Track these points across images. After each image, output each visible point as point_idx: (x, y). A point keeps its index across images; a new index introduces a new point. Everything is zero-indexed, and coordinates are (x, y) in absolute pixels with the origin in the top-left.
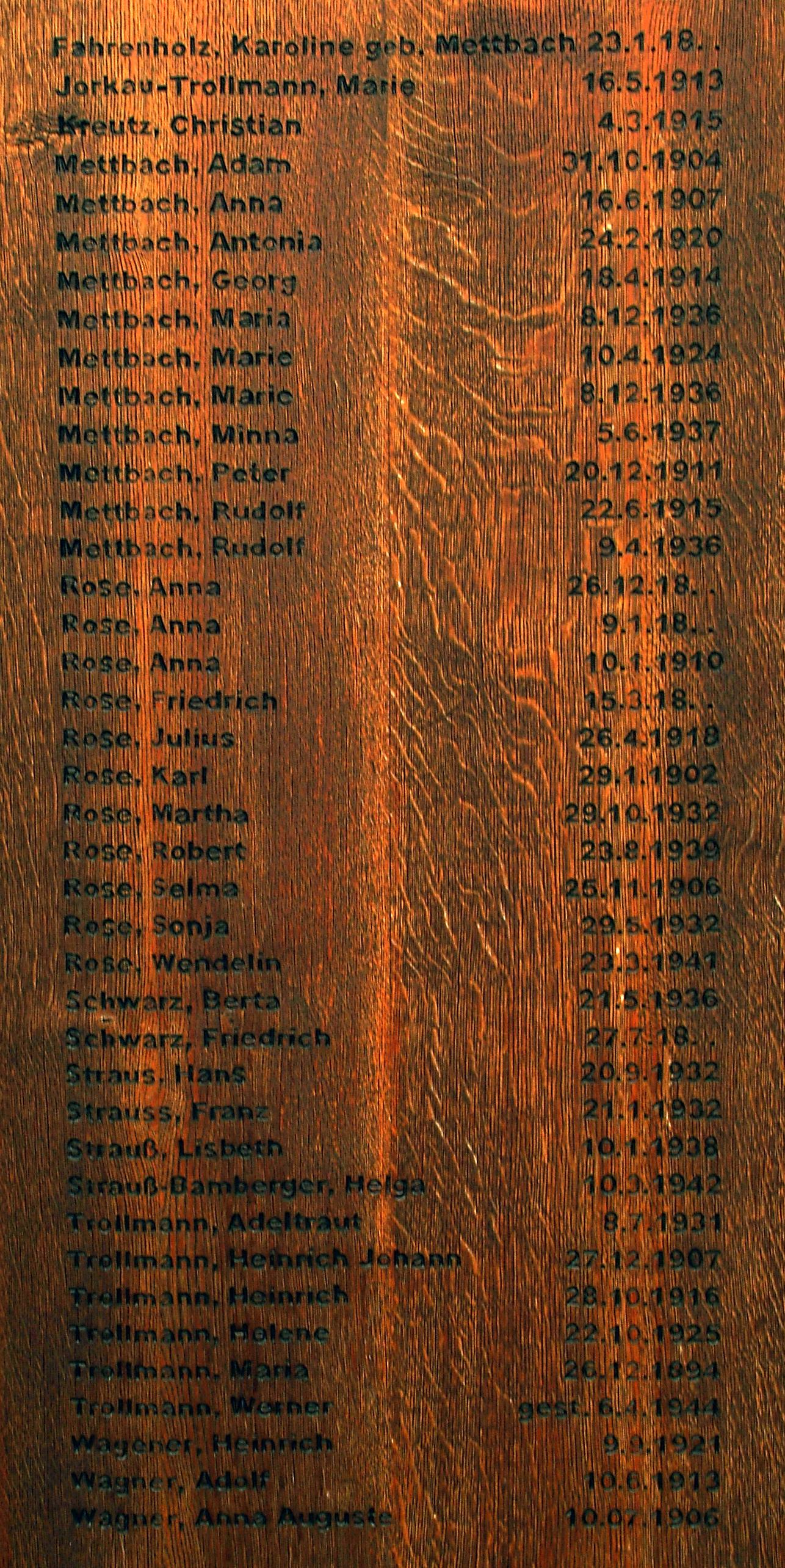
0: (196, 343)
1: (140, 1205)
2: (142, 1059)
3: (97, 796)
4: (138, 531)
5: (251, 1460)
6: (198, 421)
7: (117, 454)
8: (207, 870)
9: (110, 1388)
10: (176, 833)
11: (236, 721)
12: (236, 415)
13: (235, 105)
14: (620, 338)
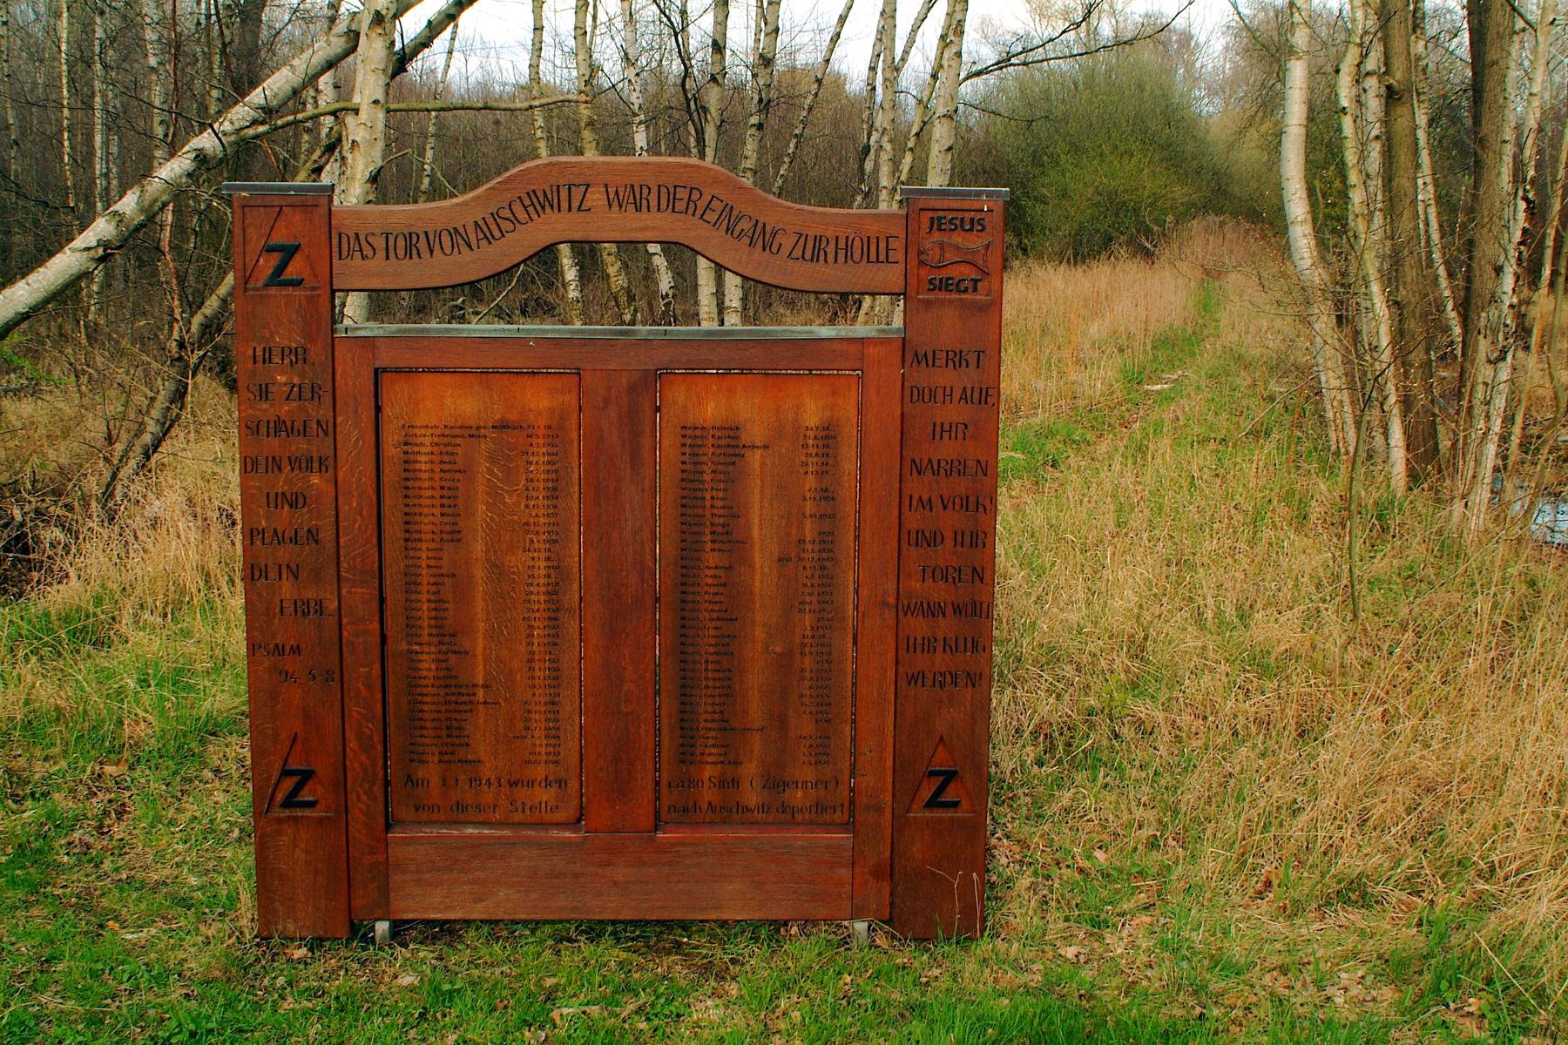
0: (437, 494)
1: (425, 691)
2: (425, 657)
3: (414, 597)
4: (422, 536)
5: (451, 749)
6: (437, 511)
7: (418, 518)
8: (441, 614)
9: (418, 732)
10: (433, 605)
11: (446, 580)
12: (446, 510)
13: (448, 440)
14: (535, 494)
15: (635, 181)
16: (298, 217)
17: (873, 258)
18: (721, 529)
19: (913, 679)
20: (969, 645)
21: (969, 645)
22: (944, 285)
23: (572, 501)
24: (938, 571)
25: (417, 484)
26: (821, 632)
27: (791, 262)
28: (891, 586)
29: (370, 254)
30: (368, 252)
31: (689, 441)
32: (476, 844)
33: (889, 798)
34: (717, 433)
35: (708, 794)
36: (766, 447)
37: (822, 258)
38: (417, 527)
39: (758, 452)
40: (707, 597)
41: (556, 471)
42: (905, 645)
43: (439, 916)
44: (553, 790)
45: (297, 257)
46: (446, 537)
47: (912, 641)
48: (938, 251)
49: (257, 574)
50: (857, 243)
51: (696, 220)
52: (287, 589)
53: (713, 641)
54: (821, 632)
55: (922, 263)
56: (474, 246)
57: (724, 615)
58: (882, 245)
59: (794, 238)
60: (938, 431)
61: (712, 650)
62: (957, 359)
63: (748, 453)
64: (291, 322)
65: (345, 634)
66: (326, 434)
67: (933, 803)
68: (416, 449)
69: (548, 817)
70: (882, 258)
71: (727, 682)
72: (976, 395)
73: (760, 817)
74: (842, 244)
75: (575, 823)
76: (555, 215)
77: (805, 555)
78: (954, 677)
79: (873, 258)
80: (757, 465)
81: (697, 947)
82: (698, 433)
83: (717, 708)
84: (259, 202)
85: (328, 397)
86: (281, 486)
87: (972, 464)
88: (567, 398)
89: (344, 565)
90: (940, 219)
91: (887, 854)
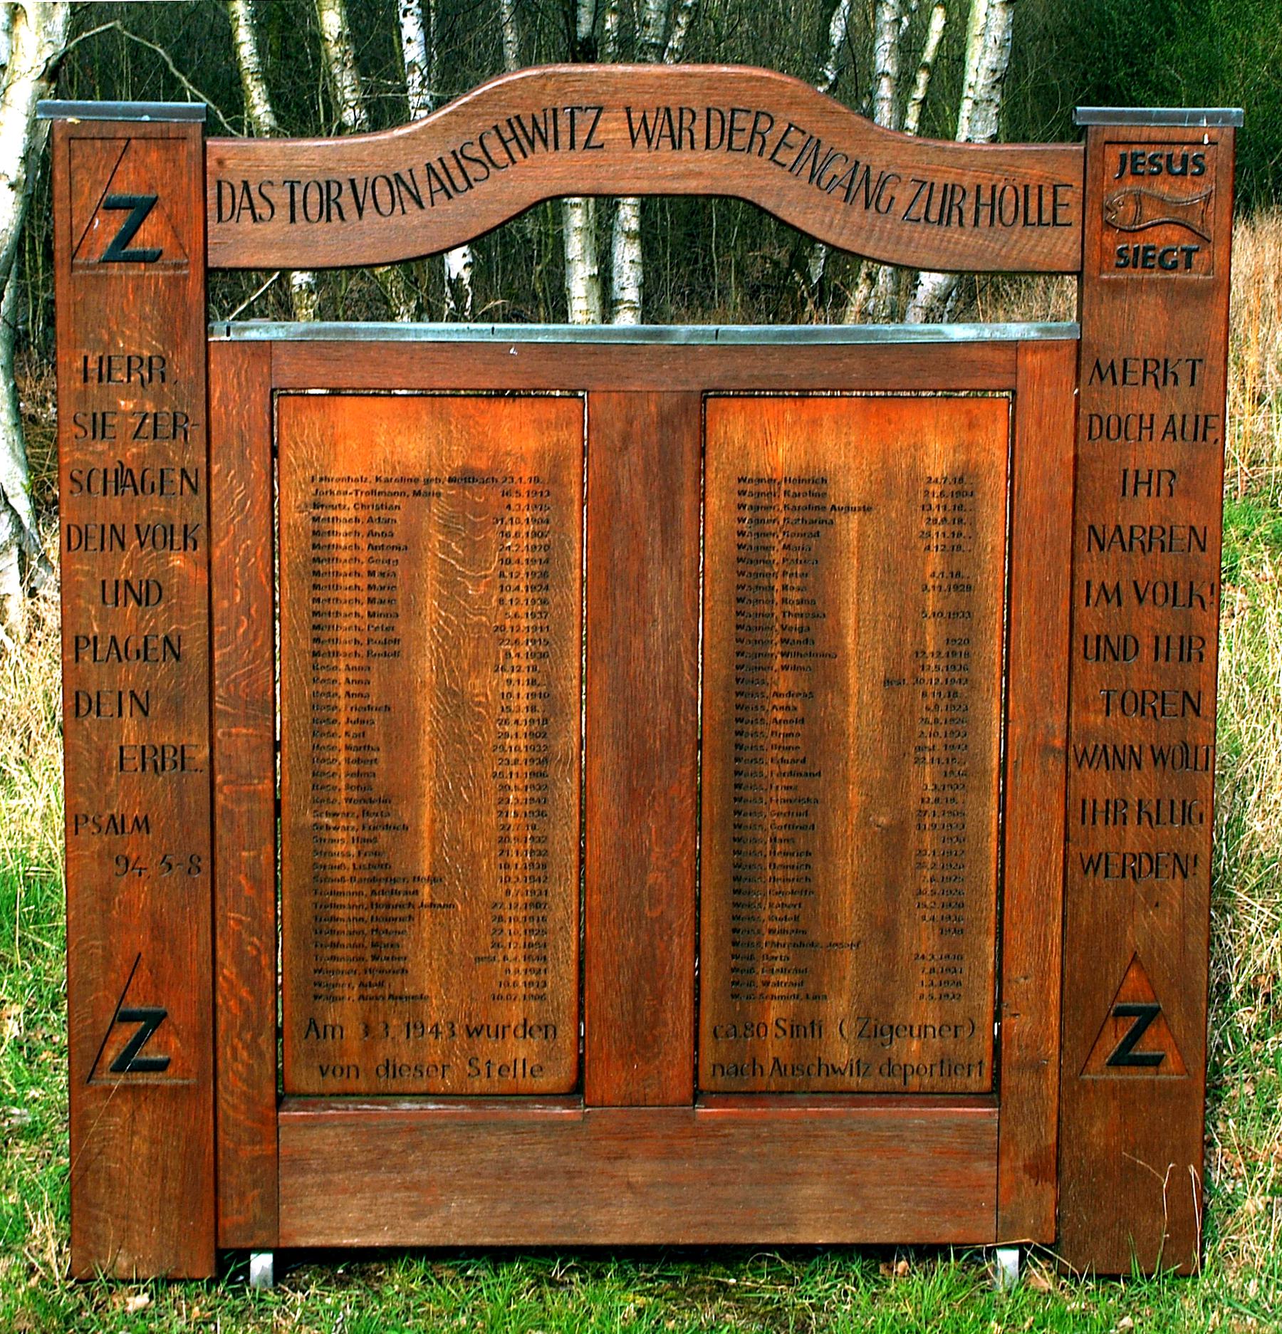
0: (363, 583)
1: (339, 887)
2: (341, 835)
3: (325, 742)
4: (340, 648)
5: (378, 978)
6: (363, 609)
7: (333, 620)
8: (366, 768)
9: (328, 952)
10: (354, 755)
11: (375, 716)
12: (376, 608)
13: (378, 500)
14: (513, 583)
15: (672, 101)
16: (154, 156)
17: (1033, 217)
18: (796, 636)
19: (1091, 865)
20: (1178, 813)
21: (1178, 813)
22: (1142, 258)
23: (572, 596)
24: (1130, 698)
25: (332, 567)
26: (949, 793)
27: (908, 226)
28: (1057, 722)
29: (266, 212)
30: (263, 210)
31: (748, 501)
32: (414, 1128)
33: (1053, 1049)
34: (793, 489)
35: (774, 1047)
36: (866, 509)
37: (955, 218)
38: (331, 634)
39: (854, 518)
40: (774, 741)
41: (547, 548)
42: (1078, 813)
43: (355, 1241)
44: (535, 1042)
45: (153, 217)
46: (376, 649)
47: (1089, 806)
48: (1132, 207)
49: (84, 705)
50: (1009, 195)
51: (764, 161)
52: (130, 730)
53: (783, 808)
54: (949, 793)
55: (1108, 225)
56: (426, 202)
57: (801, 768)
58: (1047, 199)
59: (911, 191)
60: (1131, 483)
61: (781, 821)
62: (1160, 372)
63: (840, 519)
64: (143, 318)
65: (220, 798)
66: (195, 490)
67: (1121, 1059)
68: (332, 513)
69: (526, 1084)
70: (1047, 217)
71: (803, 872)
72: (1189, 427)
73: (854, 1082)
74: (986, 197)
75: (576, 1091)
76: (551, 155)
77: (926, 675)
78: (1155, 862)
79: (1033, 217)
80: (853, 535)
81: (750, 1290)
82: (764, 487)
83: (790, 913)
84: (94, 132)
85: (198, 434)
86: (123, 570)
87: (1181, 532)
88: (564, 435)
89: (220, 692)
90: (1135, 156)
91: (1052, 1139)
